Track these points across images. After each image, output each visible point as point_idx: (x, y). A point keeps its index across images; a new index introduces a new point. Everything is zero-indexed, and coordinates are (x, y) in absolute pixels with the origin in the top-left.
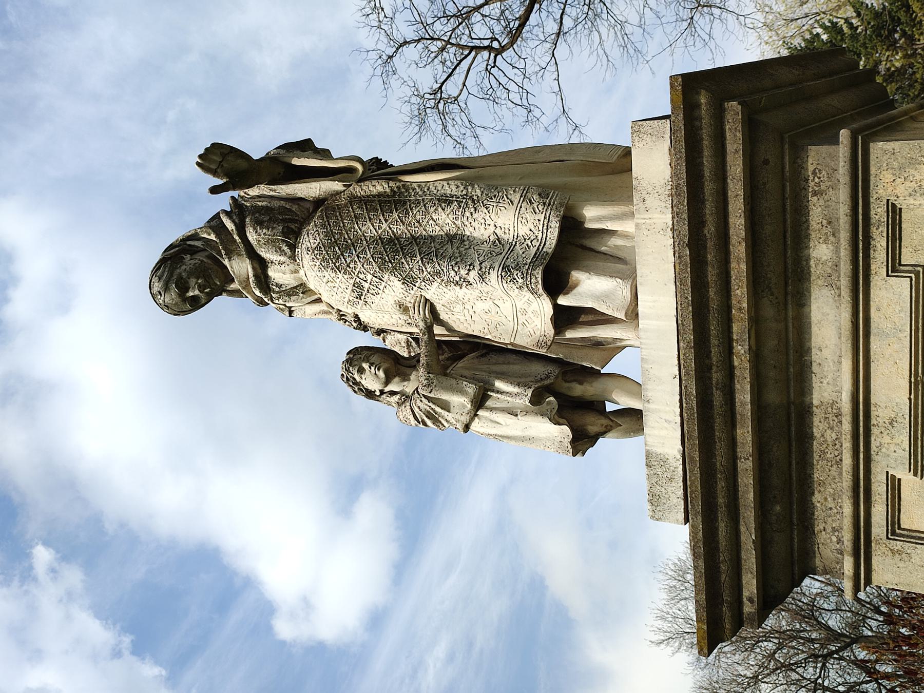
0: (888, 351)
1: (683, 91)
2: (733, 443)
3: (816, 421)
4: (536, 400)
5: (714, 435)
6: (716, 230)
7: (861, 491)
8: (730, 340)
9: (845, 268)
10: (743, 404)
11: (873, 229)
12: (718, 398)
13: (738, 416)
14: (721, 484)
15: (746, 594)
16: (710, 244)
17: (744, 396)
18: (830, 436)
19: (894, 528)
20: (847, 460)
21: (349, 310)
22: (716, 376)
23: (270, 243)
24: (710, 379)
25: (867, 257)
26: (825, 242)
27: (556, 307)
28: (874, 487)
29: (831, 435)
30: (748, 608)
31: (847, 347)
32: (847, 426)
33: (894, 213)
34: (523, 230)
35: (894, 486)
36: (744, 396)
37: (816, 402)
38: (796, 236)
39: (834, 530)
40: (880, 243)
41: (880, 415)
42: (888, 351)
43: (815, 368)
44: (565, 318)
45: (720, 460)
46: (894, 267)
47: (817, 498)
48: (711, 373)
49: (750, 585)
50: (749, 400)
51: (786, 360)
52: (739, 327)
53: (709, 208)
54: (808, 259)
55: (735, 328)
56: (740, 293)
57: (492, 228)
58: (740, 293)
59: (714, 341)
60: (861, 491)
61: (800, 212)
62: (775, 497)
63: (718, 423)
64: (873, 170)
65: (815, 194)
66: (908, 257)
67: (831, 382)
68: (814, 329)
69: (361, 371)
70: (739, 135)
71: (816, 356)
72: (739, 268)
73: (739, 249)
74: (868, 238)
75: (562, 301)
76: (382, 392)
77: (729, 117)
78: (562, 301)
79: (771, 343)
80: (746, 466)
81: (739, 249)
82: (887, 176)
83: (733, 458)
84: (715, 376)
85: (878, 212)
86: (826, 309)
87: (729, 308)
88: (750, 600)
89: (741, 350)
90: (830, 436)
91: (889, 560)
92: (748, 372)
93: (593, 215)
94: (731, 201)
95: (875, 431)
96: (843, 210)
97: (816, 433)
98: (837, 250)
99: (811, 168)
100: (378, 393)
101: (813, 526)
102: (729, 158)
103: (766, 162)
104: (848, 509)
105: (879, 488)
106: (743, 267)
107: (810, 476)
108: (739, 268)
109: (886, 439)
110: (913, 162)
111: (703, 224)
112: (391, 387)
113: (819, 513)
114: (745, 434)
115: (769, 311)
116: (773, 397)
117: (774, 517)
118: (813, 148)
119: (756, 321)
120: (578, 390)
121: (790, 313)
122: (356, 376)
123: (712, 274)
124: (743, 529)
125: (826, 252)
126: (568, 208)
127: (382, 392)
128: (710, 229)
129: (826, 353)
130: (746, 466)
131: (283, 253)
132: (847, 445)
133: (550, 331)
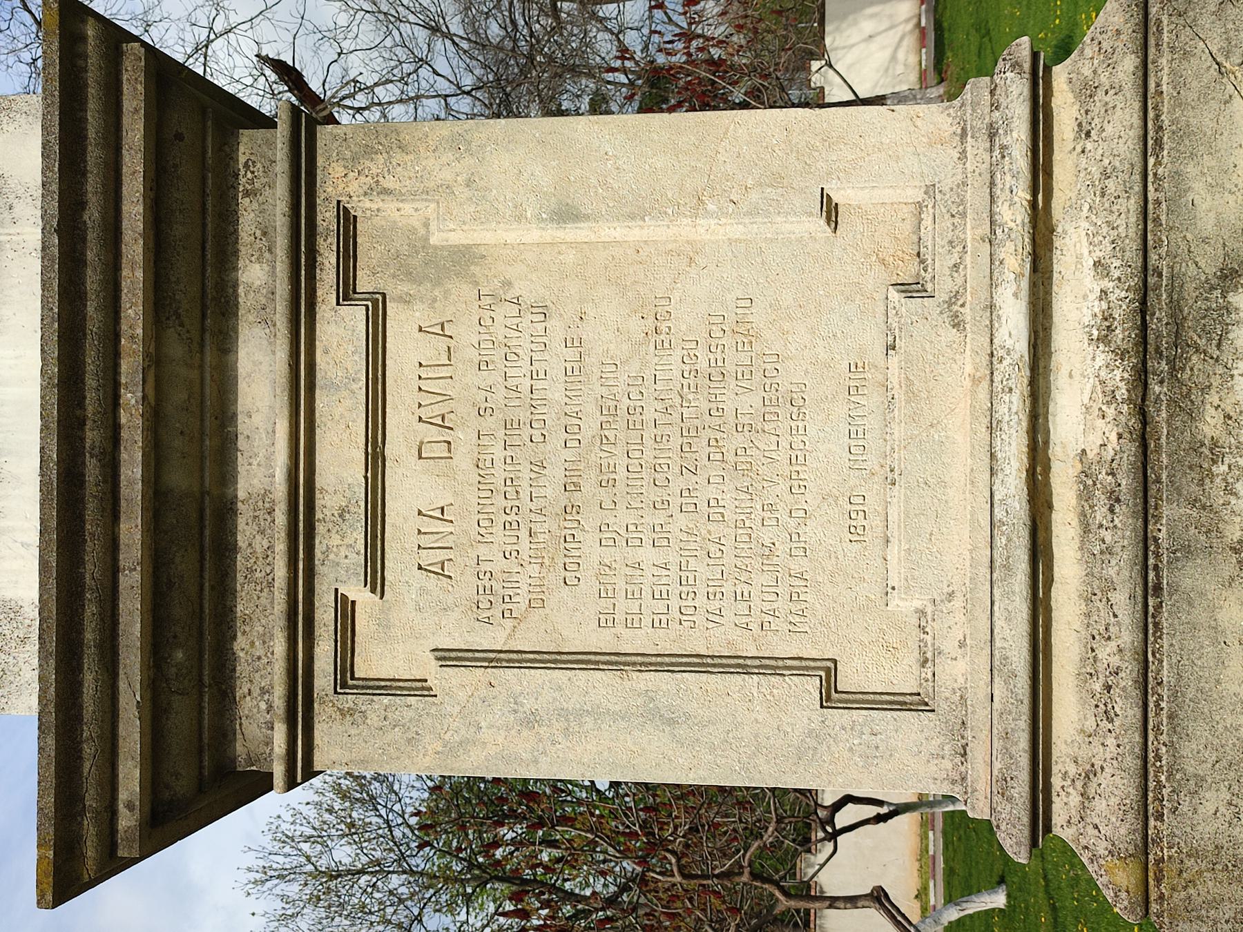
0: (338, 410)
1: (60, 10)
2: (113, 546)
3: (241, 522)
5: (83, 528)
6: (103, 218)
7: (300, 621)
8: (116, 385)
9: (283, 289)
10: (131, 483)
11: (320, 240)
12: (92, 470)
13: (123, 503)
14: (91, 609)
15: (123, 796)
16: (91, 236)
17: (132, 470)
18: (260, 543)
19: (345, 676)
20: (281, 572)
22: (92, 436)
24: (83, 439)
25: (311, 278)
26: (259, 260)
28: (318, 615)
29: (260, 542)
30: (127, 821)
31: (283, 400)
32: (281, 518)
35: (346, 611)
36: (132, 470)
37: (241, 494)
38: (221, 251)
39: (263, 691)
40: (328, 258)
41: (327, 504)
42: (338, 410)
43: (241, 443)
45: (92, 569)
46: (347, 292)
47: (240, 643)
48: (83, 430)
49: (130, 779)
50: (139, 476)
51: (199, 425)
52: (130, 366)
53: (93, 184)
54: (235, 286)
55: (124, 366)
56: (133, 313)
58: (133, 313)
59: (91, 382)
60: (300, 621)
61: (228, 218)
62: (175, 637)
63: (91, 509)
64: (320, 161)
65: (247, 194)
66: (364, 284)
67: (261, 467)
68: (242, 386)
70: (140, 88)
71: (244, 425)
72: (134, 277)
73: (134, 249)
74: (312, 252)
77: (128, 64)
79: (178, 396)
80: (131, 581)
81: (134, 249)
82: (337, 170)
83: (113, 570)
84: (89, 434)
85: (326, 217)
86: (259, 356)
87: (117, 336)
88: (130, 806)
89: (131, 398)
90: (260, 543)
91: (337, 727)
92: (139, 432)
94: (126, 180)
95: (320, 529)
97: (242, 541)
98: (273, 273)
99: (242, 159)
101: (233, 690)
102: (126, 120)
103: (179, 137)
104: (279, 646)
105: (325, 615)
106: (139, 274)
107: (232, 610)
108: (134, 277)
109: (335, 540)
111: (82, 205)
113: (242, 669)
114: (132, 531)
115: (175, 349)
116: (178, 478)
117: (174, 670)
118: (246, 132)
119: (155, 362)
121: (208, 358)
123: (92, 280)
124: (122, 685)
125: (259, 275)
128: (92, 214)
129: (257, 419)
130: (131, 581)
132: (281, 547)
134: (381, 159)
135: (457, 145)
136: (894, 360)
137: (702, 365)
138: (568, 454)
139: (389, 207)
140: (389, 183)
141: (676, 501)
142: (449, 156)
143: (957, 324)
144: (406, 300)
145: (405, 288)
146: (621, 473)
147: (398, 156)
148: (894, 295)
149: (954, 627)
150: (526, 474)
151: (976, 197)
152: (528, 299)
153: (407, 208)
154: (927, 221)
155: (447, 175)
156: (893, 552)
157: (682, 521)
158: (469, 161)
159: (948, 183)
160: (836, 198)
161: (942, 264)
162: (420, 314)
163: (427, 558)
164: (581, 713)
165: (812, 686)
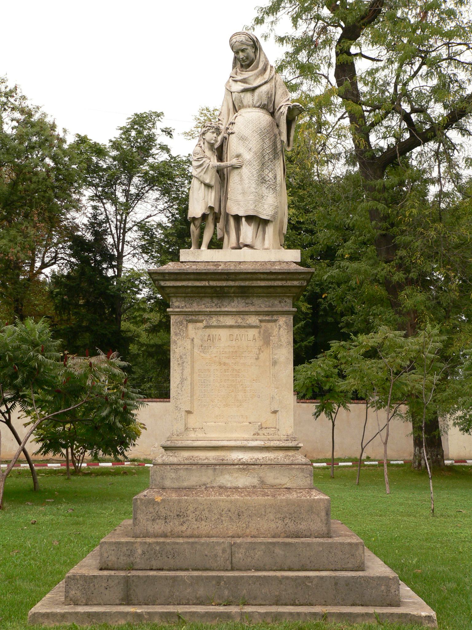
4: (211, 208)
21: (235, 128)
23: (260, 98)
27: (242, 217)
33: (275, 321)
34: (266, 206)
35: (202, 321)
44: (237, 218)
46: (261, 321)
57: (267, 195)
66: (263, 324)
69: (213, 132)
74: (268, 315)
75: (243, 219)
76: (204, 139)
78: (243, 219)
82: (284, 319)
83: (208, 280)
85: (275, 317)
93: (270, 230)
96: (276, 309)
100: (204, 137)
110: (287, 325)
112: (206, 143)
120: (210, 219)
122: (211, 131)
126: (272, 221)
127: (204, 139)
131: (257, 103)
133: (233, 214)
134: (286, 328)
135: (289, 343)
136: (248, 424)
137: (247, 389)
138: (231, 364)
139: (277, 329)
140: (281, 329)
141: (222, 384)
142: (286, 341)
143: (254, 435)
144: (260, 332)
145: (262, 331)
146: (227, 373)
147: (286, 331)
148: (259, 424)
149: (200, 435)
150: (227, 355)
151: (276, 437)
152: (260, 356)
153: (277, 333)
154: (273, 429)
155: (283, 341)
156: (213, 423)
157: (218, 385)
158: (285, 345)
159: (279, 433)
160: (277, 413)
161: (265, 431)
162: (257, 335)
163: (211, 336)
164: (183, 366)
165: (189, 409)
